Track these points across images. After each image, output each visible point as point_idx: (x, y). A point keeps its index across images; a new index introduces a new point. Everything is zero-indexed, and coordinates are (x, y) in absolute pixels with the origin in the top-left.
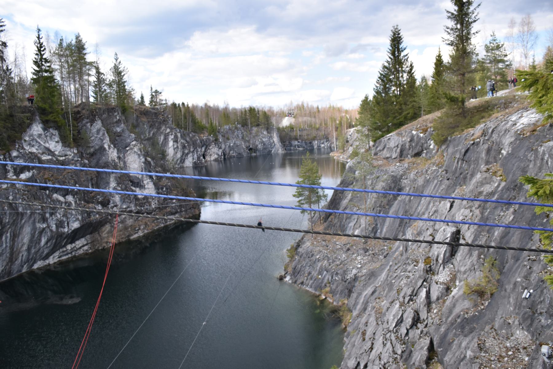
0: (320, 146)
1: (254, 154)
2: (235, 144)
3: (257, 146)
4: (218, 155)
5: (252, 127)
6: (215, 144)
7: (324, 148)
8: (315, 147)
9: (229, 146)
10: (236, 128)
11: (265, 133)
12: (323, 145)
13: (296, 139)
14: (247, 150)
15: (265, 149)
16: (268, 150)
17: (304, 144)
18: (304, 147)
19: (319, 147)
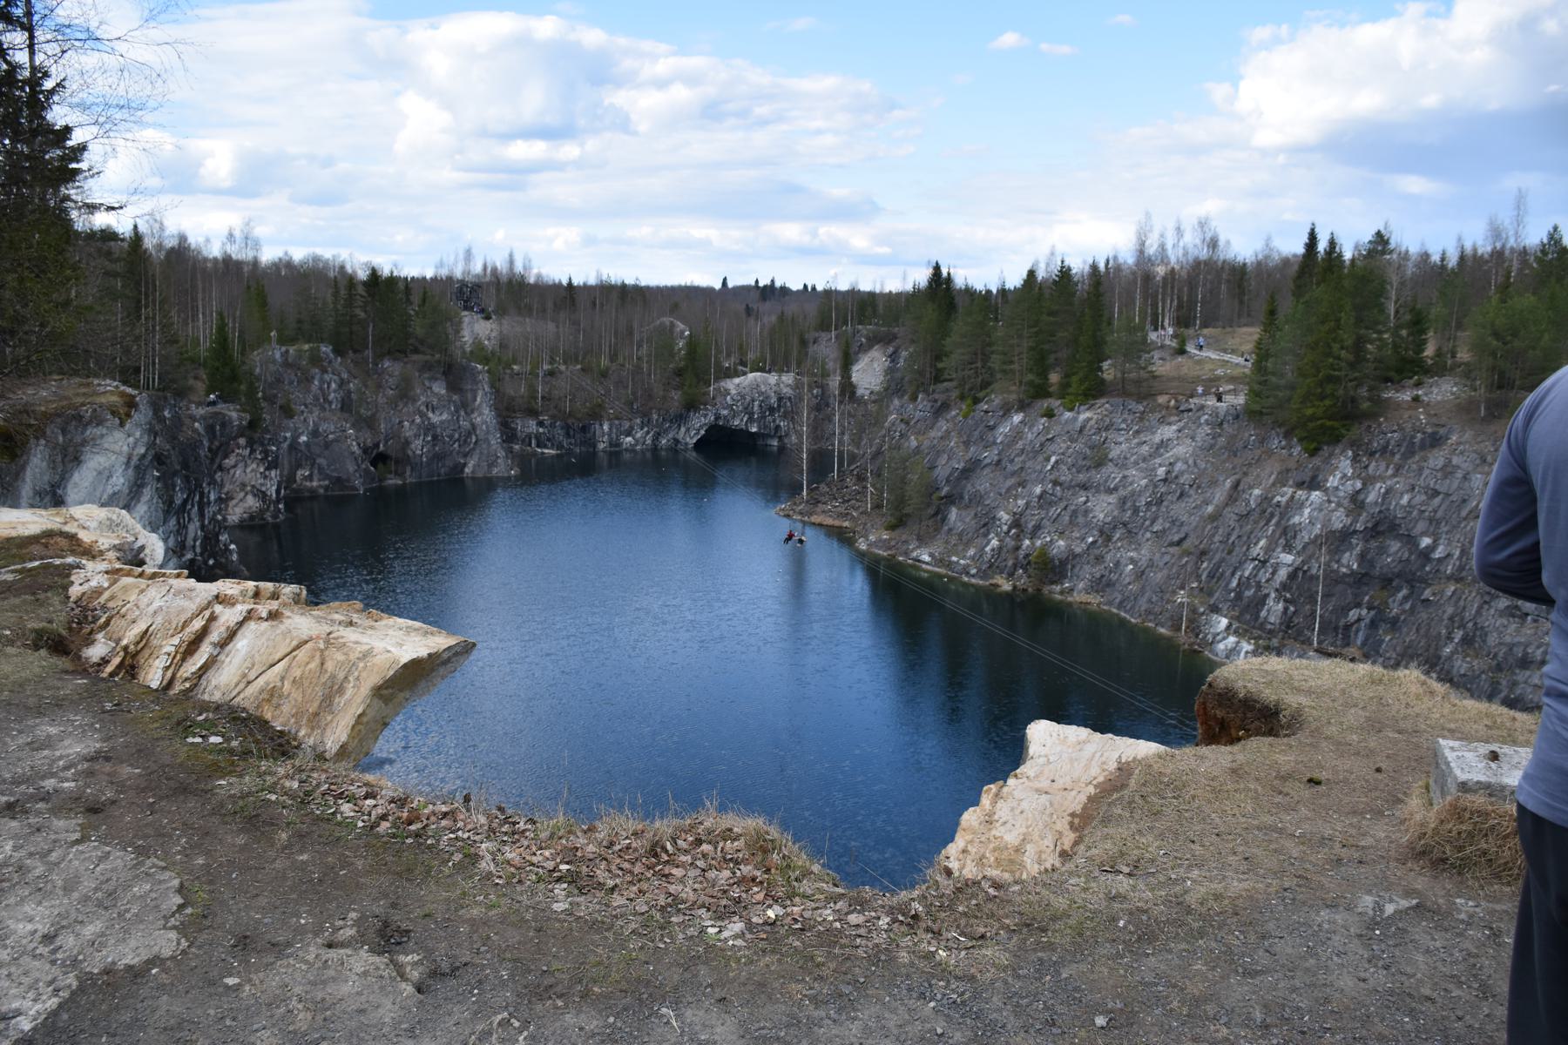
0: (618, 445)
1: (393, 481)
2: (315, 433)
3: (407, 443)
4: (261, 495)
5: (379, 357)
6: (251, 443)
7: (631, 450)
8: (601, 446)
10: (316, 360)
11: (439, 388)
12: (629, 439)
13: (532, 413)
14: (366, 465)
15: (438, 457)
16: (449, 463)
17: (559, 433)
18: (560, 447)
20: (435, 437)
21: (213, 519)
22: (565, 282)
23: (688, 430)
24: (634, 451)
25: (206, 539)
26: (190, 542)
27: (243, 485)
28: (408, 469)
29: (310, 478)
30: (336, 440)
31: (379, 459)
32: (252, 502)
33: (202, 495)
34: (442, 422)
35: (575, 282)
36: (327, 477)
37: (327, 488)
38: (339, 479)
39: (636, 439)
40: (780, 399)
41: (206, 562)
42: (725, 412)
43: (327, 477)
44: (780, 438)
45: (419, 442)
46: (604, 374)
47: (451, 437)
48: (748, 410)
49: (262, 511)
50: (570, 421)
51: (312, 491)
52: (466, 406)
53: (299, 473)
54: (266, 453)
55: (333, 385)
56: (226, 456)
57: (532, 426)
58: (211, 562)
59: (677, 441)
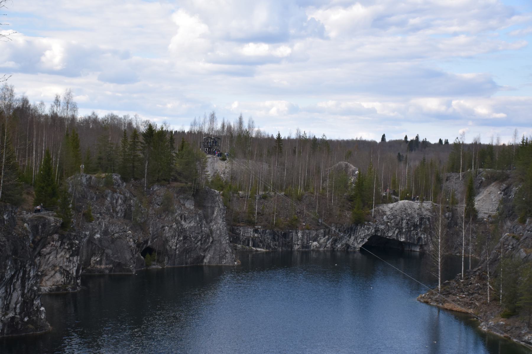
0: (308, 247)
1: (156, 266)
2: (105, 233)
3: (167, 241)
5: (151, 183)
6: (62, 238)
7: (317, 251)
8: (296, 247)
10: (109, 184)
11: (190, 205)
12: (315, 243)
13: (251, 223)
14: (138, 255)
15: (187, 251)
16: (194, 255)
17: (268, 238)
18: (268, 247)
19: (306, 246)
20: (185, 238)
21: (31, 289)
22: (275, 137)
23: (356, 239)
24: (318, 251)
25: (24, 303)
26: (12, 305)
27: (54, 266)
28: (166, 258)
29: (100, 262)
30: (119, 238)
31: (147, 251)
32: (59, 278)
33: (25, 272)
34: (190, 228)
35: (283, 137)
36: (112, 262)
37: (111, 270)
38: (119, 264)
39: (320, 243)
40: (421, 219)
41: (22, 319)
42: (382, 227)
43: (112, 262)
44: (421, 246)
45: (174, 241)
46: (300, 199)
47: (196, 238)
48: (398, 226)
49: (65, 284)
50: (275, 230)
51: (101, 271)
52: (207, 218)
53: (93, 259)
54: (72, 245)
55: (120, 201)
56: (44, 246)
57: (250, 232)
58: (26, 319)
59: (348, 246)
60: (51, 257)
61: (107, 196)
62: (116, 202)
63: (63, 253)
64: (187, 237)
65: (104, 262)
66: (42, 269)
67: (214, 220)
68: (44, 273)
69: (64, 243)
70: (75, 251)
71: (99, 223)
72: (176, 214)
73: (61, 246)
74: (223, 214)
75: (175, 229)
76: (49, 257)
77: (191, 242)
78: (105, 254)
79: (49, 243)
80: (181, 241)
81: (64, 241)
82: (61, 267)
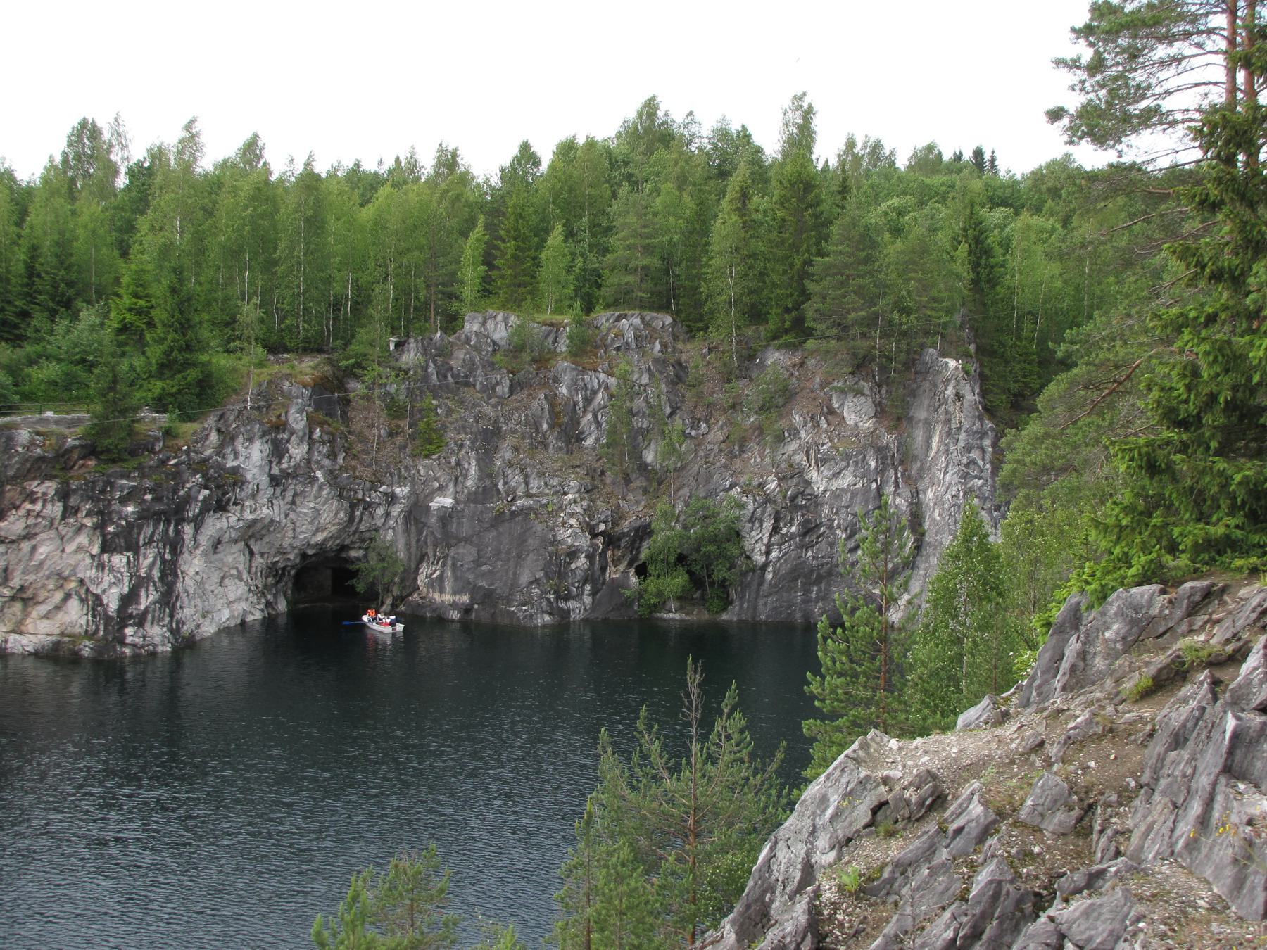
2: (486, 492)
4: (94, 603)
9: (416, 513)
20: (808, 529)
27: (62, 578)
29: (438, 584)
34: (837, 495)
37: (467, 610)
53: (424, 570)
60: (43, 550)
61: (556, 380)
62: (588, 401)
63: (83, 539)
64: (818, 526)
65: (448, 585)
66: (16, 582)
67: (930, 469)
68: (28, 594)
69: (76, 511)
70: (116, 535)
71: (458, 464)
72: (794, 446)
73: (64, 517)
74: (968, 448)
75: (768, 500)
76: (34, 549)
77: (832, 545)
78: (449, 562)
79: (17, 508)
80: (792, 537)
81: (73, 501)
82: (82, 582)
